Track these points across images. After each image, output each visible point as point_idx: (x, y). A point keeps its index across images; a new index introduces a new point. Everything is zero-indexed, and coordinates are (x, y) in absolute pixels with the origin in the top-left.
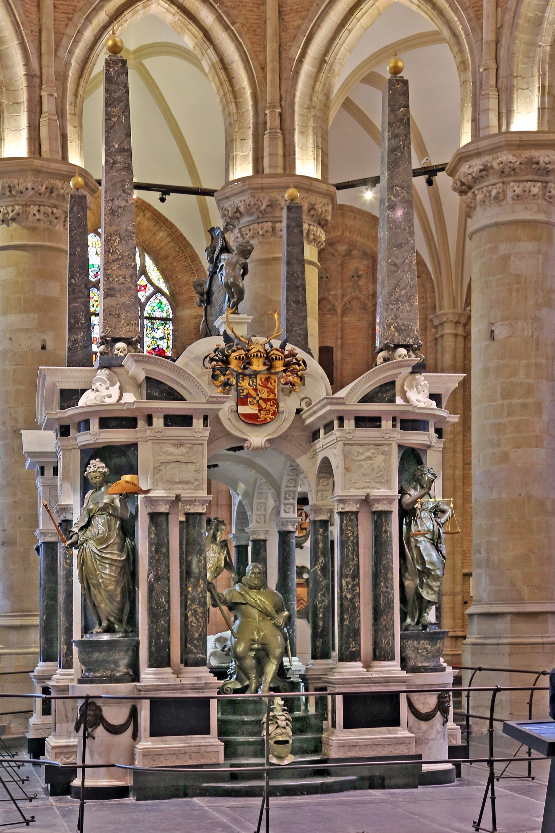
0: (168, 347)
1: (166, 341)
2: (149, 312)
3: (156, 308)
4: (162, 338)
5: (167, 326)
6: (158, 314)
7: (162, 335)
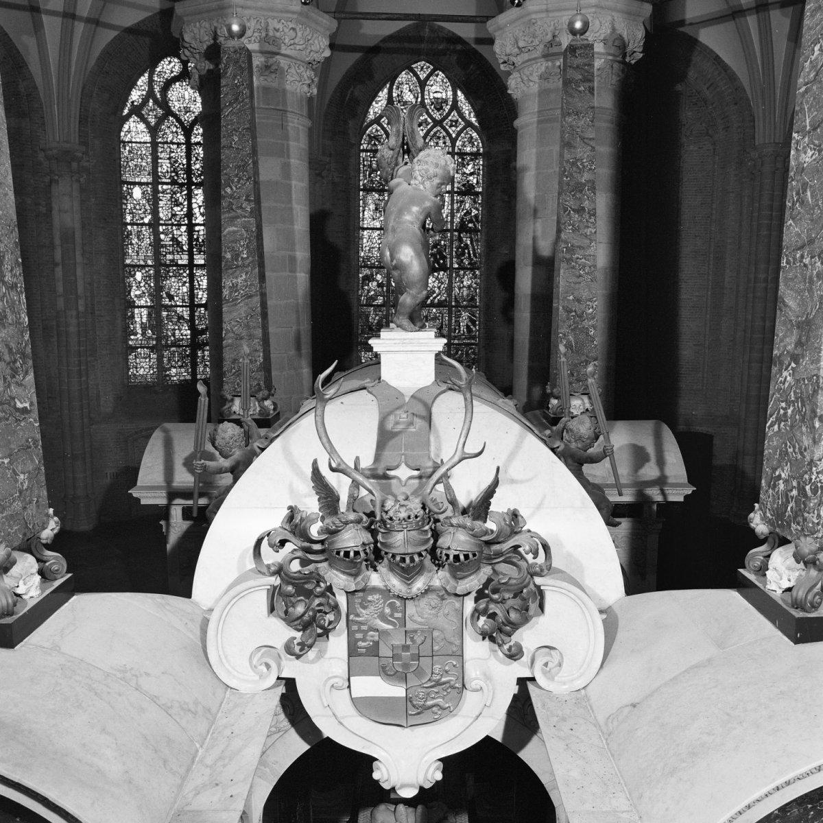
0: (478, 182)
1: (475, 176)
2: (460, 147)
3: (467, 143)
4: (472, 174)
5: (477, 161)
6: (468, 149)
7: (472, 171)
